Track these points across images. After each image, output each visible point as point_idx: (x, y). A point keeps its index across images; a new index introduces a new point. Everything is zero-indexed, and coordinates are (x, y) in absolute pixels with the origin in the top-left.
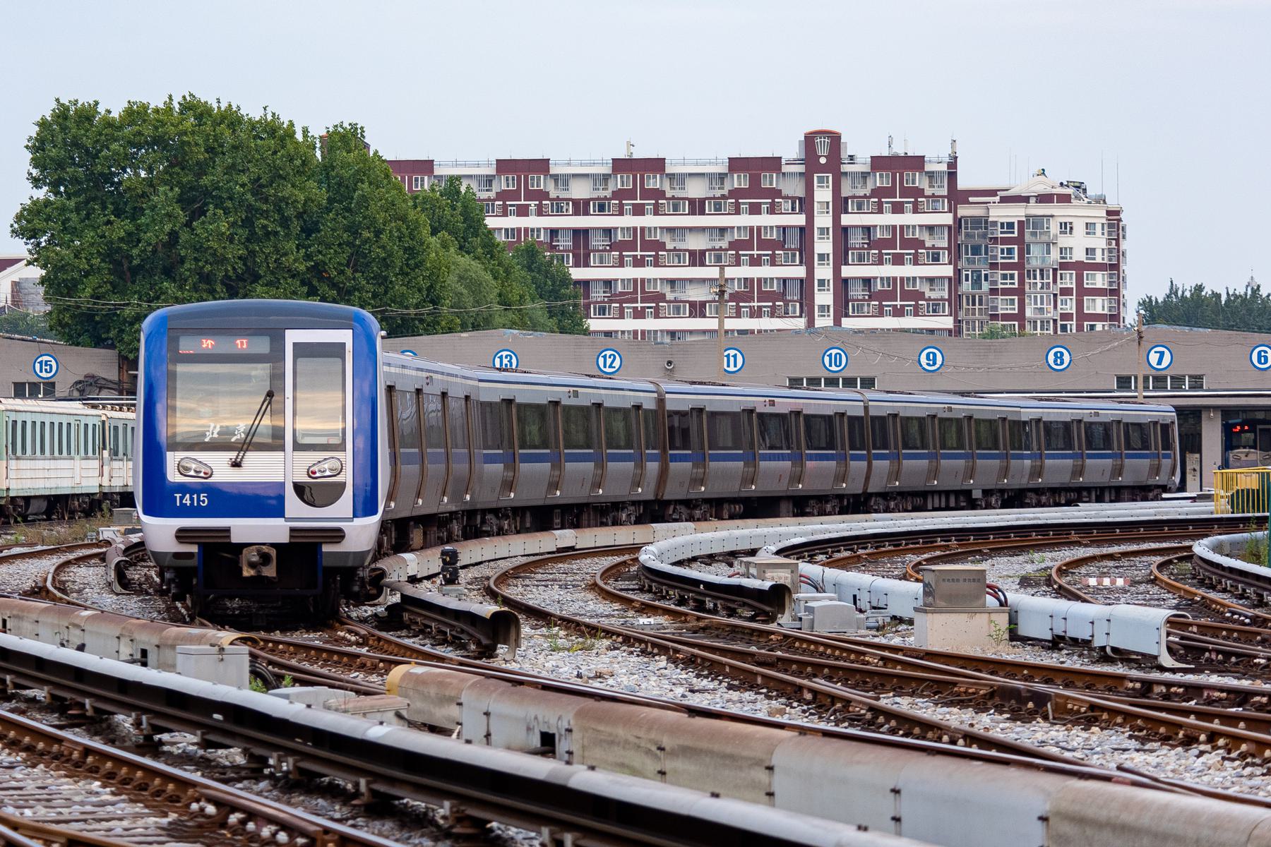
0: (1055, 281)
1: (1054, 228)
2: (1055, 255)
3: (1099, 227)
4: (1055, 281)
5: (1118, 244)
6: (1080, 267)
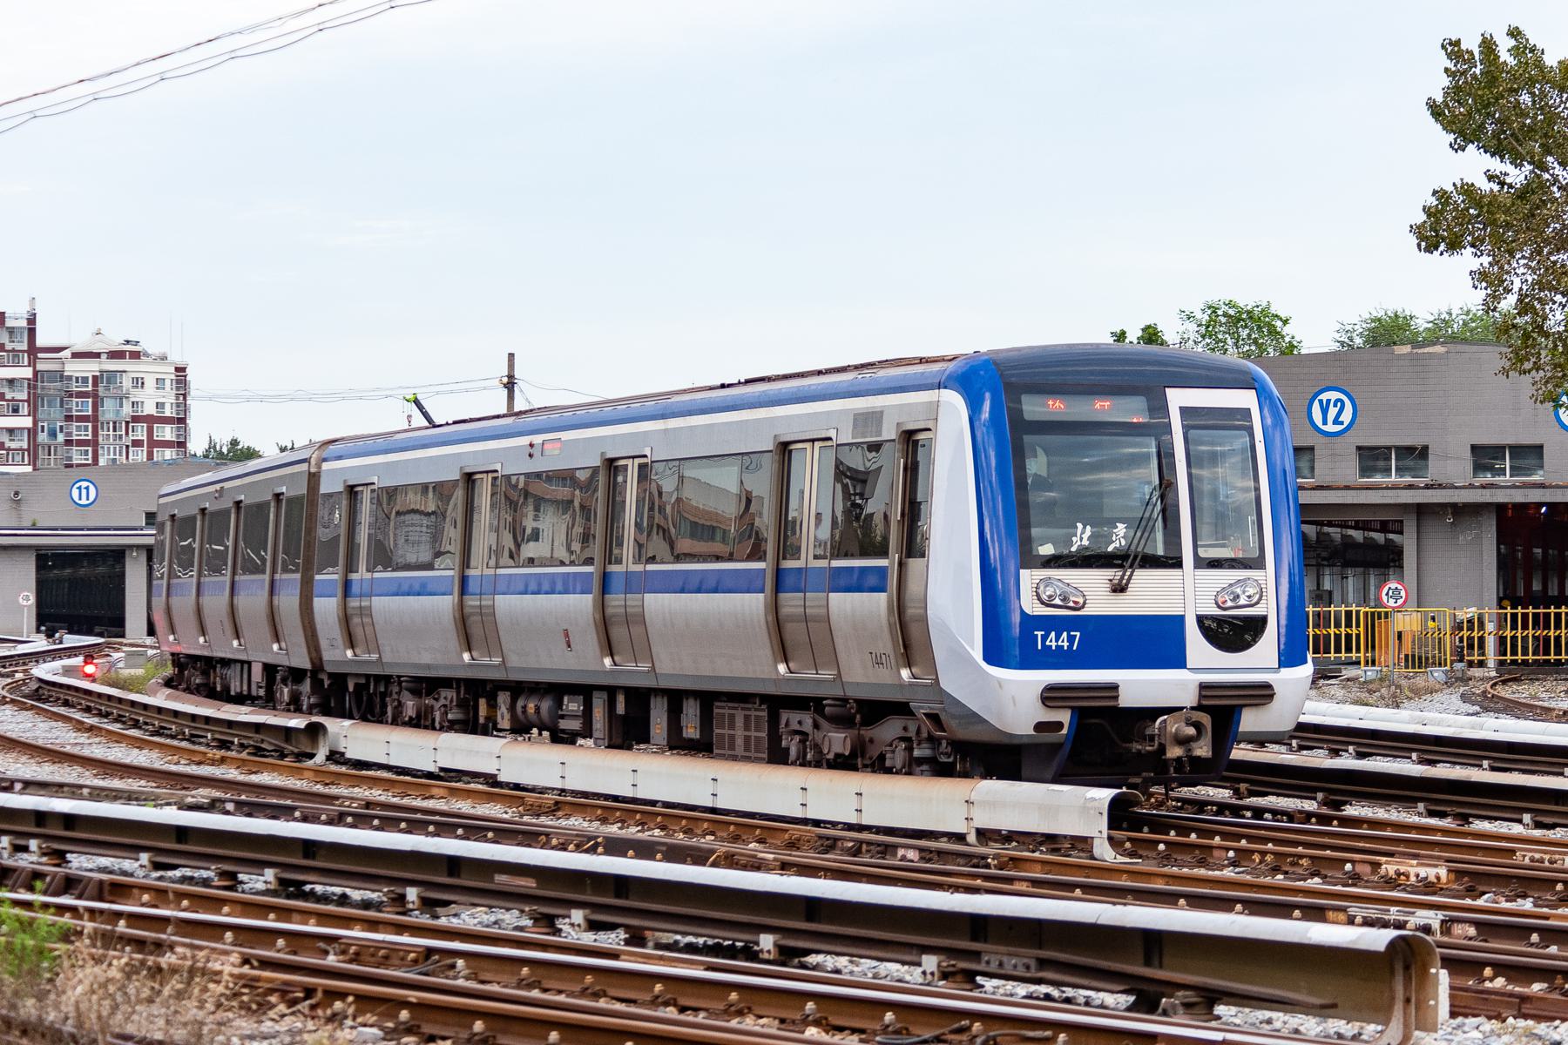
0: (127, 433)
1: (127, 382)
2: (127, 410)
3: (168, 383)
4: (127, 433)
5: (185, 399)
6: (150, 420)
